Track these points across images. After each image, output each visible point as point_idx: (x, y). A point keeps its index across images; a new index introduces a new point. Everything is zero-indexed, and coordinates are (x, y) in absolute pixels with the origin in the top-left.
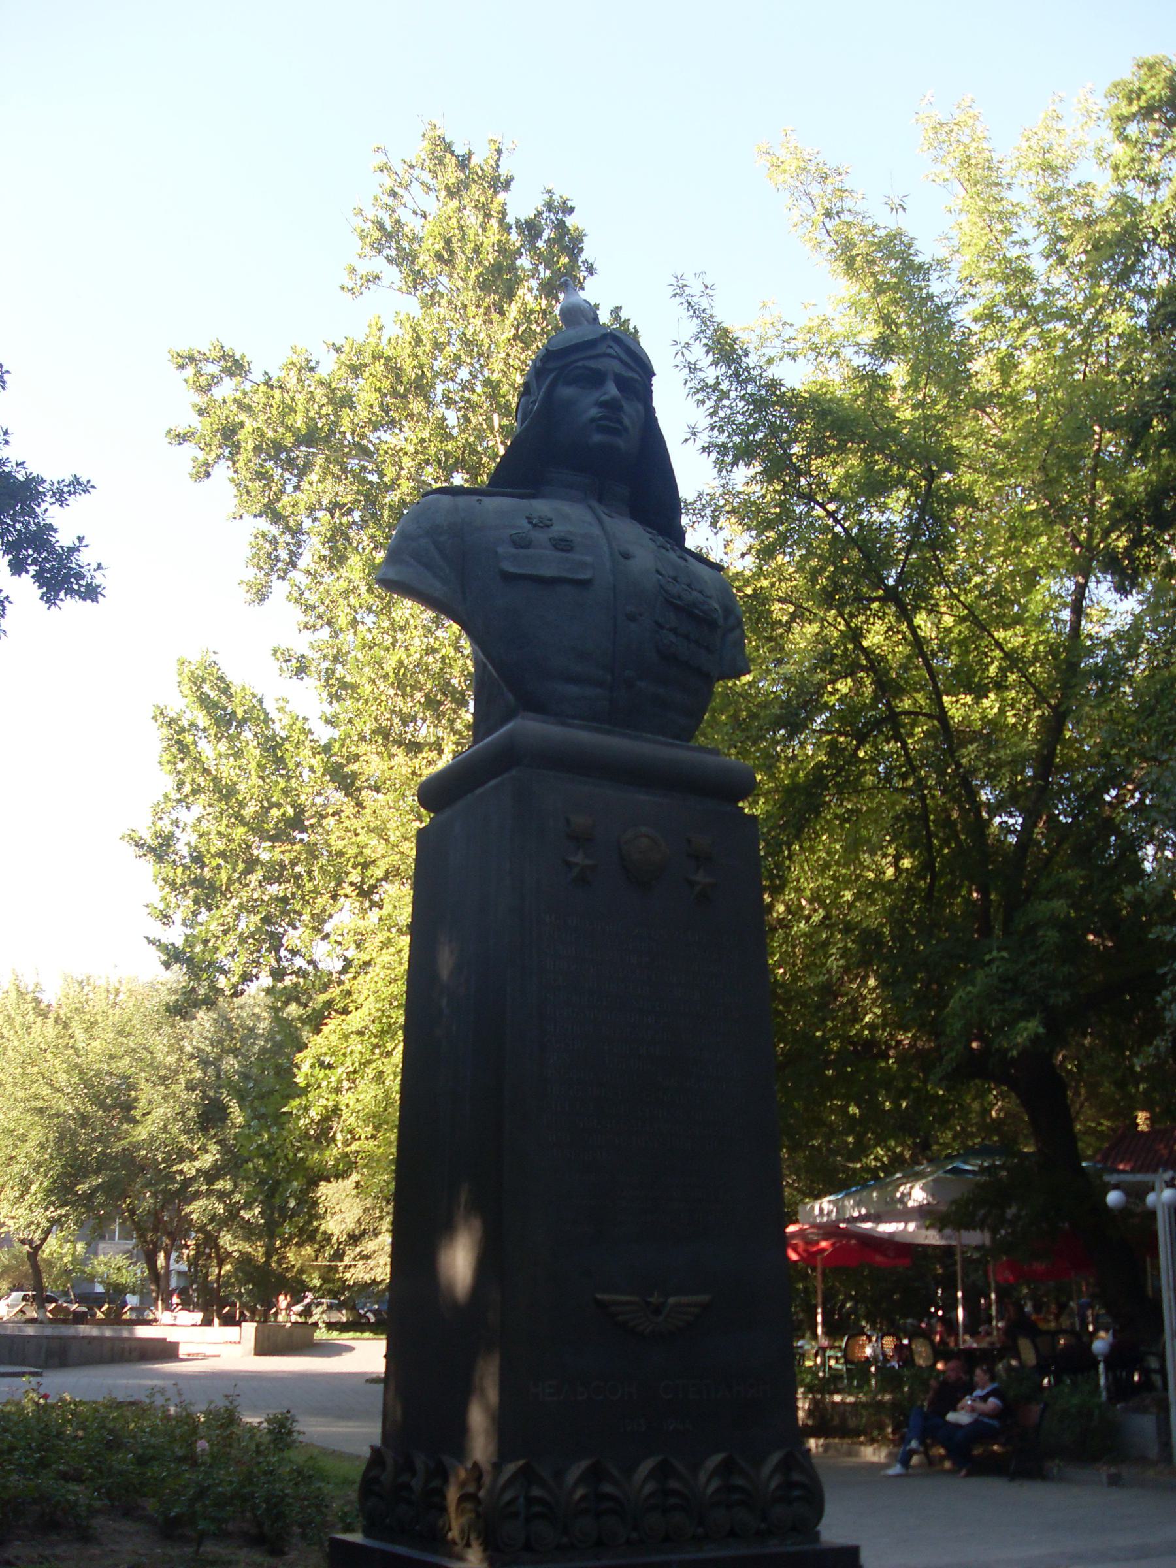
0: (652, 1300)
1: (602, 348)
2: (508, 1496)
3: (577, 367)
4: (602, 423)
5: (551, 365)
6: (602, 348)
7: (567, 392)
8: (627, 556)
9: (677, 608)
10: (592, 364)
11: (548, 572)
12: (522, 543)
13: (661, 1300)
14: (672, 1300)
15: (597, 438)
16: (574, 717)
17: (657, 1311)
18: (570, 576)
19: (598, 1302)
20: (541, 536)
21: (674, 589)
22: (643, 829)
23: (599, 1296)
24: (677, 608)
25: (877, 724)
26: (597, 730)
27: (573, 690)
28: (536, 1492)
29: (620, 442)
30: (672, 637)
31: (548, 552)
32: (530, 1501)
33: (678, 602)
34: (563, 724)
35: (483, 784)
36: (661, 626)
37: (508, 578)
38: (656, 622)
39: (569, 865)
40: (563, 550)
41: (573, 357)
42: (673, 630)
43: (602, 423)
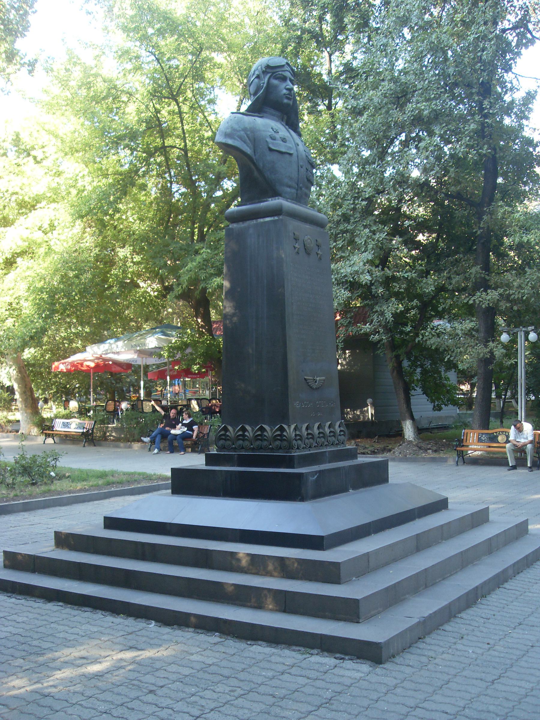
7: (275, 82)
11: (283, 150)
15: (286, 101)
20: (277, 136)
25: (156, 149)
27: (288, 190)
28: (298, 433)
37: (271, 150)
39: (295, 248)
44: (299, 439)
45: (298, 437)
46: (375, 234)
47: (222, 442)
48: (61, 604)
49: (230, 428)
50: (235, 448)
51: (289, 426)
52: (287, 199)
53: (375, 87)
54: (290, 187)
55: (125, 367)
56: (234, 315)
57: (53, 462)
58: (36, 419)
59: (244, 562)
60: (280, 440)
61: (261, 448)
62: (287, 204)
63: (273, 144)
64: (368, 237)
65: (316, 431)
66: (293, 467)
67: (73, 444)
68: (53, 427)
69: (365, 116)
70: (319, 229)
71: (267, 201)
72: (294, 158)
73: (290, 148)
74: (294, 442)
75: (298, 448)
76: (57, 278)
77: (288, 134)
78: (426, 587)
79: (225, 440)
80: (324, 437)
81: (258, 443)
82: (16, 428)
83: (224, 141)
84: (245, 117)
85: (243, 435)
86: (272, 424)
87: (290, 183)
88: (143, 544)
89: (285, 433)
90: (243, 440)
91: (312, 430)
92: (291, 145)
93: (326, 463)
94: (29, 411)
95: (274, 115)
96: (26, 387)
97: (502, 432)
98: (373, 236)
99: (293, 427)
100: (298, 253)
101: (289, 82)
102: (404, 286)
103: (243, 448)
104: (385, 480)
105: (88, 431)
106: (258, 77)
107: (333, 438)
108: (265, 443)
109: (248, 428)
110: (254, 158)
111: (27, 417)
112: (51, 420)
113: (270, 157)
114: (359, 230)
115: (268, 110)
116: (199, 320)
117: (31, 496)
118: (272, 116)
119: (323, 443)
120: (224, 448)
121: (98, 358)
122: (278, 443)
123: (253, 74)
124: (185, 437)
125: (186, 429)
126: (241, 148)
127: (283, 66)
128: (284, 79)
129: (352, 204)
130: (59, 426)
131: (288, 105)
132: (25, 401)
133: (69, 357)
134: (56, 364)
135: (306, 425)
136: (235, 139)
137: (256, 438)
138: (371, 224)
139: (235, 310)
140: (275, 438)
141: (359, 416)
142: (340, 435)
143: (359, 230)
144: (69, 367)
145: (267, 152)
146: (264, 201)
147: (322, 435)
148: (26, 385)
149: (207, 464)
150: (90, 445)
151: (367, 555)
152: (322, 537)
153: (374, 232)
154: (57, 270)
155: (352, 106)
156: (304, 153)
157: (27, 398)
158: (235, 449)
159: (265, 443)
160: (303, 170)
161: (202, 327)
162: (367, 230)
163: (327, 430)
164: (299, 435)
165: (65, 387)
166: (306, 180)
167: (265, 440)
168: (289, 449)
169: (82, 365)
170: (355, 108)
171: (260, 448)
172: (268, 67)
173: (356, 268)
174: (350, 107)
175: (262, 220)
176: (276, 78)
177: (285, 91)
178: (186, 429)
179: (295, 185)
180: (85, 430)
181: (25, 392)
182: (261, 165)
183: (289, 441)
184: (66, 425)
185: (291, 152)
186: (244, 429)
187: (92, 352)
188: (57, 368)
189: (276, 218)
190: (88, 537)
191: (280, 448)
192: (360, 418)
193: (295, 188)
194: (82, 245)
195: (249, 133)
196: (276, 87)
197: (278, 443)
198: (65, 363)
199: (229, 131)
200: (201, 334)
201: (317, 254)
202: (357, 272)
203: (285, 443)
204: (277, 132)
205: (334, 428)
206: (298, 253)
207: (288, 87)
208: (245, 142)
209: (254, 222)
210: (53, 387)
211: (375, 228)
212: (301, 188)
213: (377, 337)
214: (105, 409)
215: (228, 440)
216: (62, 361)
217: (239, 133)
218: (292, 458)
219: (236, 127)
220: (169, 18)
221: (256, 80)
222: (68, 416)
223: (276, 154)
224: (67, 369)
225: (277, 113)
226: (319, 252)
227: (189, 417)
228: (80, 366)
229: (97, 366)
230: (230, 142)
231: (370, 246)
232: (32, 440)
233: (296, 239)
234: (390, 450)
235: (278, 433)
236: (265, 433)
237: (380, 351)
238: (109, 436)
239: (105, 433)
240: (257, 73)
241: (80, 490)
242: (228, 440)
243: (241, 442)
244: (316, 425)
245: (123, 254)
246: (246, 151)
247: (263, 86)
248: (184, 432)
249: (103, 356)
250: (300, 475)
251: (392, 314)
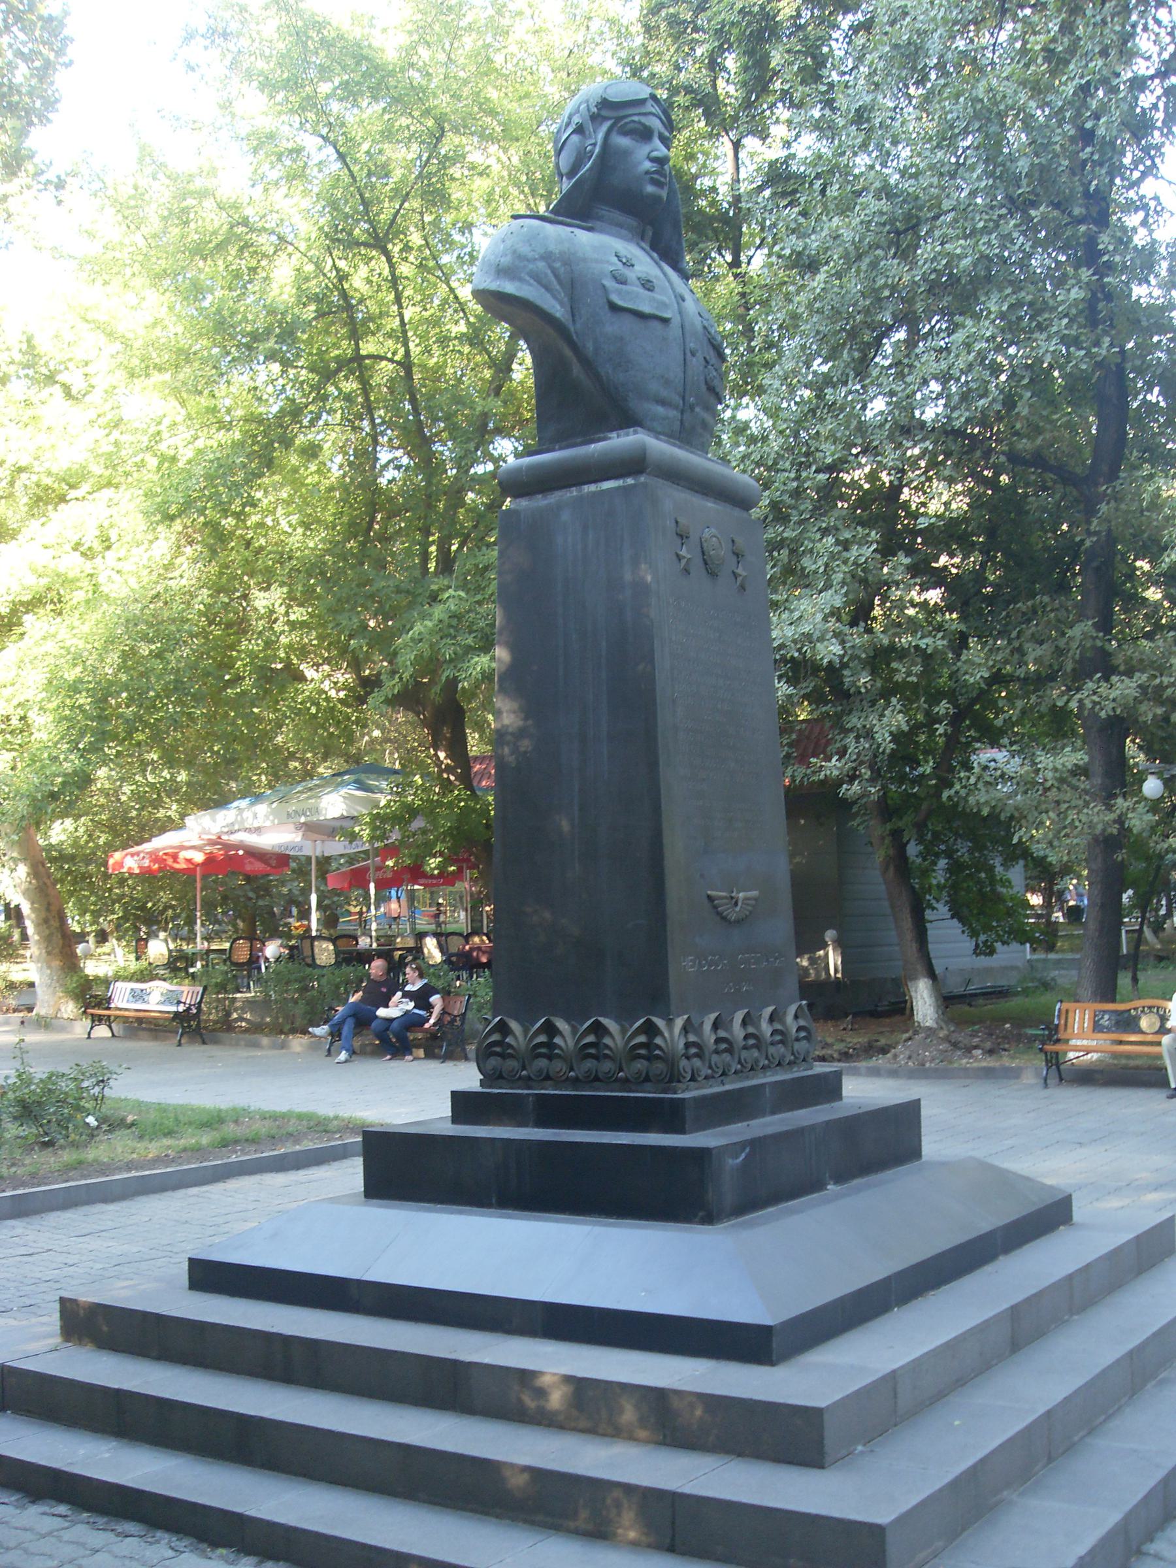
3: (634, 122)
4: (655, 176)
5: (604, 113)
7: (623, 142)
11: (646, 309)
14: (741, 895)
15: (650, 189)
18: (660, 314)
19: (709, 897)
20: (631, 275)
25: (342, 363)
26: (674, 445)
27: (660, 410)
28: (692, 1038)
34: (657, 438)
35: (595, 481)
37: (614, 308)
39: (678, 556)
40: (649, 290)
41: (630, 111)
43: (655, 176)
44: (696, 1055)
45: (693, 1051)
46: (846, 549)
47: (493, 1062)
48: (62, 1509)
49: (514, 1025)
50: (529, 1078)
51: (670, 1022)
52: (657, 434)
53: (845, 208)
54: (663, 402)
55: (274, 863)
56: (521, 733)
57: (97, 1090)
58: (72, 984)
59: (556, 1399)
60: (648, 1058)
61: (597, 1079)
62: (658, 447)
63: (619, 293)
64: (833, 556)
65: (738, 1031)
66: (681, 1130)
67: (156, 1038)
68: (109, 1000)
69: (821, 277)
70: (737, 512)
71: (605, 439)
72: (674, 330)
74: (684, 1063)
75: (693, 1079)
76: (114, 658)
77: (658, 272)
78: (1050, 1459)
79: (503, 1056)
80: (757, 1046)
81: (589, 1064)
82: (26, 1000)
83: (494, 285)
84: (547, 226)
85: (550, 1045)
86: (626, 1017)
87: (664, 393)
88: (287, 1341)
89: (658, 1041)
90: (550, 1058)
91: (729, 1028)
92: (665, 299)
93: (763, 1116)
94: (56, 963)
95: (621, 226)
96: (48, 910)
97: (1150, 1008)
98: (845, 554)
99: (679, 1022)
100: (686, 571)
101: (657, 142)
102: (917, 669)
103: (548, 1078)
104: (914, 1153)
105: (189, 1009)
106: (580, 130)
107: (782, 1049)
108: (607, 1066)
109: (562, 1025)
110: (572, 329)
111: (51, 977)
112: (106, 982)
113: (613, 326)
114: (809, 539)
115: (604, 211)
116: (442, 755)
117: (35, 1178)
118: (616, 228)
119: (757, 1061)
120: (501, 1077)
121: (212, 843)
122: (640, 1065)
123: (568, 124)
124: (410, 1022)
125: (412, 1004)
126: (539, 302)
127: (642, 102)
128: (645, 134)
129: (794, 480)
130: (122, 997)
131: (656, 199)
132: (47, 940)
133: (149, 840)
134: (118, 856)
135: (713, 1016)
136: (521, 280)
137: (583, 1052)
138: (839, 524)
139: (526, 719)
140: (633, 1053)
141: (806, 969)
142: (797, 1039)
143: (809, 539)
144: (146, 863)
145: (606, 314)
146: (599, 440)
147: (755, 1040)
148: (49, 904)
149: (457, 1118)
150: (192, 1041)
151: (892, 1378)
152: (767, 1330)
153: (846, 545)
154: (110, 641)
155: (793, 251)
156: (698, 321)
157: (51, 935)
158: (527, 1082)
159: (607, 1066)
160: (696, 363)
161: (449, 769)
162: (830, 540)
163: (766, 1029)
164: (694, 1044)
165: (143, 908)
166: (704, 388)
167: (606, 1056)
168: (670, 1081)
169: (175, 857)
170: (799, 254)
171: (594, 1079)
172: (605, 104)
173: (806, 628)
174: (787, 252)
175: (592, 488)
176: (625, 133)
177: (647, 165)
178: (412, 1004)
179: (677, 399)
180: (181, 1008)
181: (46, 921)
182: (590, 346)
183: (670, 1061)
184: (137, 996)
185: (666, 315)
186: (550, 1029)
187: (198, 829)
188: (120, 864)
189: (630, 481)
190: (145, 1315)
191: (647, 1079)
192: (808, 975)
193: (676, 408)
194: (172, 583)
195: (557, 265)
196: (626, 153)
197: (640, 1065)
198: (138, 854)
199: (506, 260)
200: (447, 786)
201: (735, 575)
202: (808, 637)
203: (659, 1066)
204: (629, 264)
205: (783, 1023)
206: (686, 571)
207: (655, 154)
208: (547, 288)
209: (574, 492)
210: (117, 906)
211: (847, 535)
212: (692, 408)
213: (856, 787)
214: (230, 958)
215: (511, 1056)
216: (131, 850)
217: (531, 266)
218: (677, 1107)
219: (525, 250)
220: (366, 58)
221: (575, 138)
222: (146, 975)
223: (628, 322)
224: (140, 867)
225: (632, 222)
226: (740, 571)
227: (421, 976)
228: (170, 862)
229: (210, 860)
230: (509, 287)
231: (838, 577)
232: (62, 1029)
233: (682, 536)
234: (884, 1051)
235: (642, 1039)
236: (607, 1040)
237: (858, 820)
238: (236, 1020)
239: (228, 1014)
240: (576, 119)
241: (157, 1161)
242: (511, 1056)
243: (542, 1063)
244: (739, 1016)
245: (265, 603)
246: (552, 311)
247: (592, 152)
248: (407, 1013)
249: (225, 837)
250: (701, 1156)
251: (891, 733)
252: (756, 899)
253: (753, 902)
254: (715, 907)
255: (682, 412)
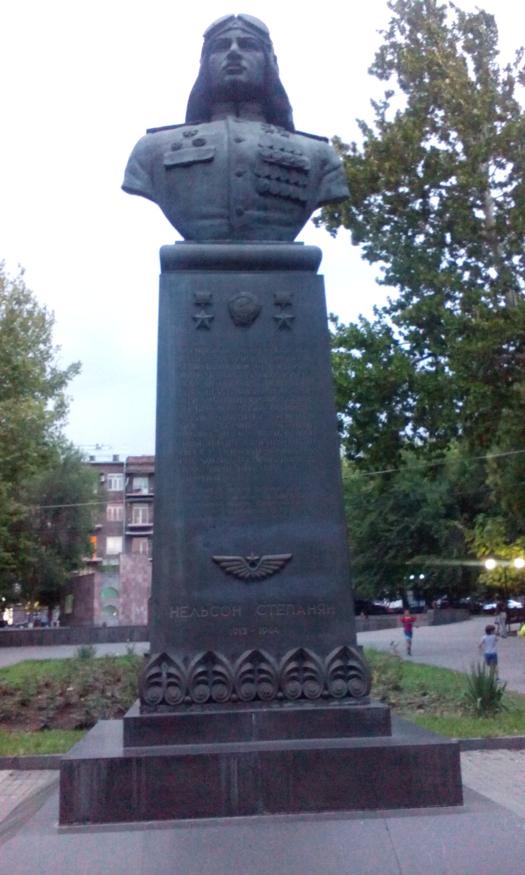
0: (249, 558)
1: (230, 25)
2: (154, 671)
6: (230, 25)
8: (239, 141)
9: (271, 164)
10: (223, 36)
12: (177, 147)
13: (256, 558)
14: (265, 557)
15: (227, 78)
16: (208, 239)
17: (253, 564)
21: (267, 152)
22: (243, 293)
23: (216, 557)
24: (271, 164)
29: (242, 77)
30: (266, 181)
31: (191, 149)
32: (170, 675)
33: (272, 160)
36: (259, 176)
37: (169, 168)
38: (256, 174)
39: (195, 319)
42: (268, 177)
43: (230, 68)
73: (209, 151)
166: (257, 196)
179: (223, 211)
193: (221, 216)
206: (203, 326)
212: (240, 213)
252: (287, 561)
253: (281, 563)
254: (223, 568)
255: (228, 218)
